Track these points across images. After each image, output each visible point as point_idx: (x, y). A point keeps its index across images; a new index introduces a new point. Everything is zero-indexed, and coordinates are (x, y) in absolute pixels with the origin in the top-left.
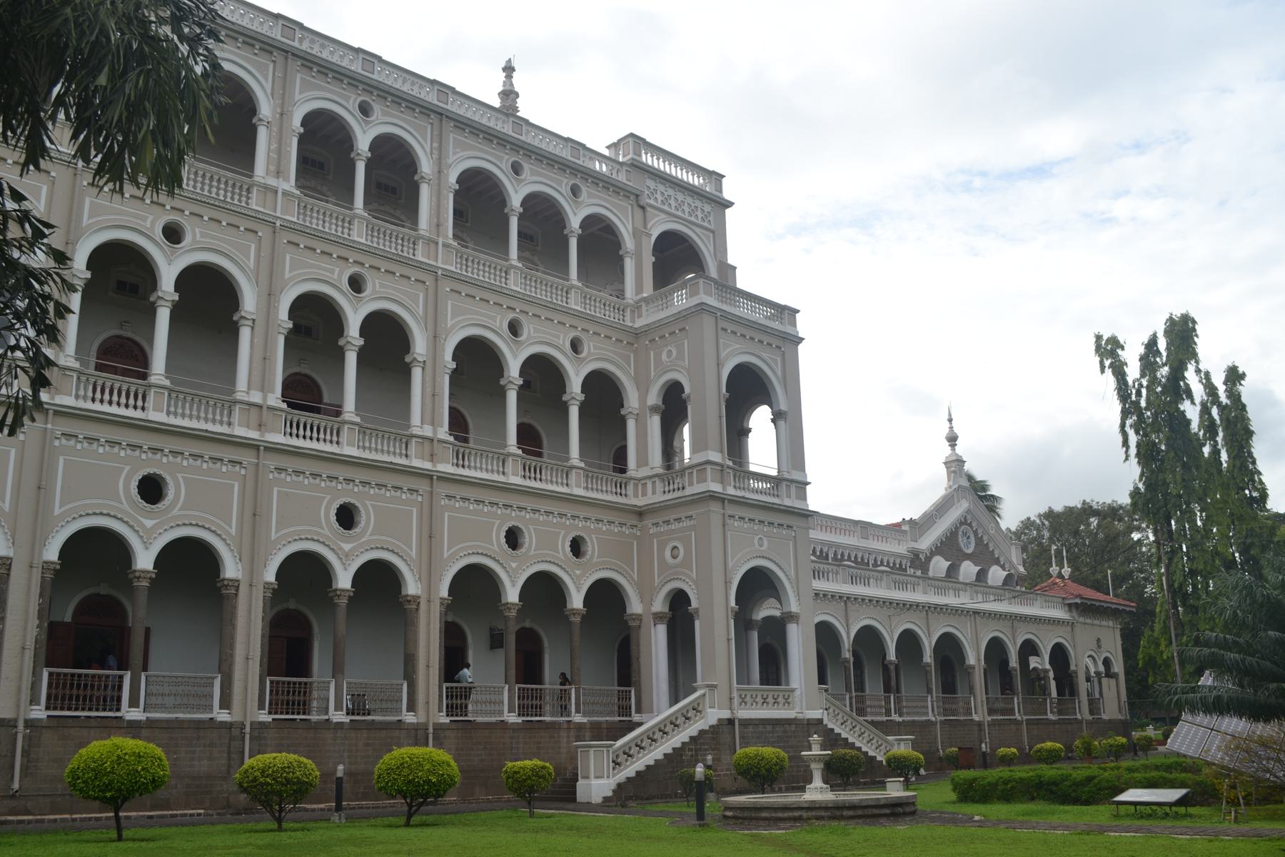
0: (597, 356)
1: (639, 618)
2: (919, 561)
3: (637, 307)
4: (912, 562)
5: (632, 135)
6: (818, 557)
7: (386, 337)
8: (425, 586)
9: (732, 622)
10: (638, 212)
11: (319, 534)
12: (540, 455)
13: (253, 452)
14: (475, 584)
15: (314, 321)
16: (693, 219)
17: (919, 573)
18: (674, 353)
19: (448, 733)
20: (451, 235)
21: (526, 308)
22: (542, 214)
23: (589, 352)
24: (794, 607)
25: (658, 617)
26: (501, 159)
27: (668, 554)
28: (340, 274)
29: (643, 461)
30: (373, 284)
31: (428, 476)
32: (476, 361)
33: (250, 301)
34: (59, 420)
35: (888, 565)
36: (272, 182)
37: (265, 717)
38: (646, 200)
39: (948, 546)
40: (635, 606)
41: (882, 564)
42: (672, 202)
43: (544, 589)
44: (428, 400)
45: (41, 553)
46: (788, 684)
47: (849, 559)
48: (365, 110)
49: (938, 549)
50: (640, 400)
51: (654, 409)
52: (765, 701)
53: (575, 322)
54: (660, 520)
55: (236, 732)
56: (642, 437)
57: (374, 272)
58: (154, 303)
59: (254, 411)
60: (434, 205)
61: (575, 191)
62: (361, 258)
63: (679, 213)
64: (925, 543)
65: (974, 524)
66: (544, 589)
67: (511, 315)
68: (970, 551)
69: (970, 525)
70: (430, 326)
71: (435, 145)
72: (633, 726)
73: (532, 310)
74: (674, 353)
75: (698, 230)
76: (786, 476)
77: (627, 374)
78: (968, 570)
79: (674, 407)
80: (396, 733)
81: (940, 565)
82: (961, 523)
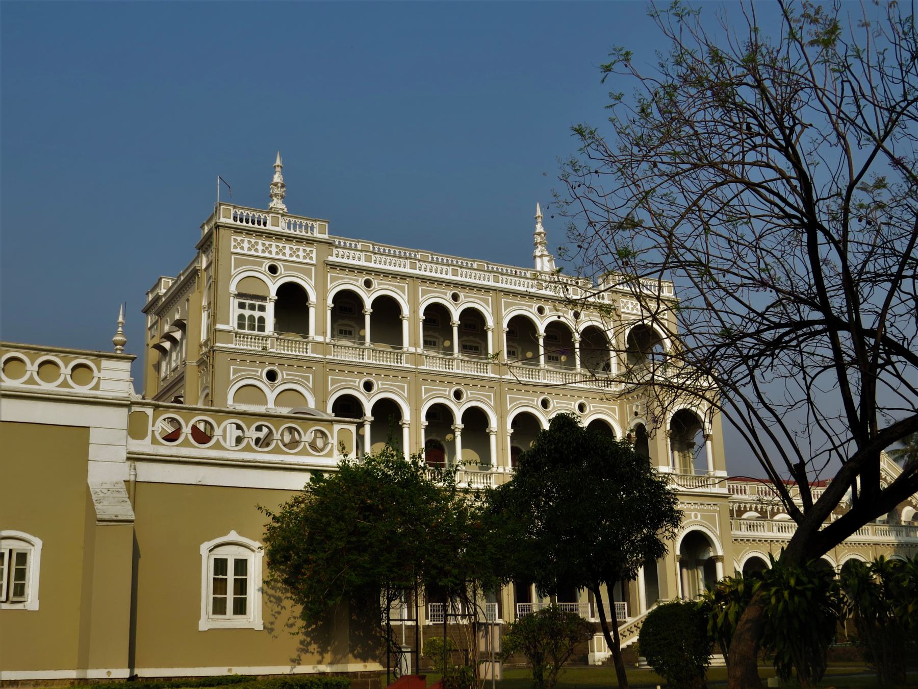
6: (759, 513)
7: (476, 421)
9: (678, 564)
15: (439, 417)
22: (558, 332)
23: (590, 411)
24: (720, 552)
26: (531, 307)
37: (428, 622)
48: (455, 297)
53: (580, 394)
60: (496, 340)
62: (459, 381)
72: (625, 622)
73: (554, 391)
77: (614, 419)
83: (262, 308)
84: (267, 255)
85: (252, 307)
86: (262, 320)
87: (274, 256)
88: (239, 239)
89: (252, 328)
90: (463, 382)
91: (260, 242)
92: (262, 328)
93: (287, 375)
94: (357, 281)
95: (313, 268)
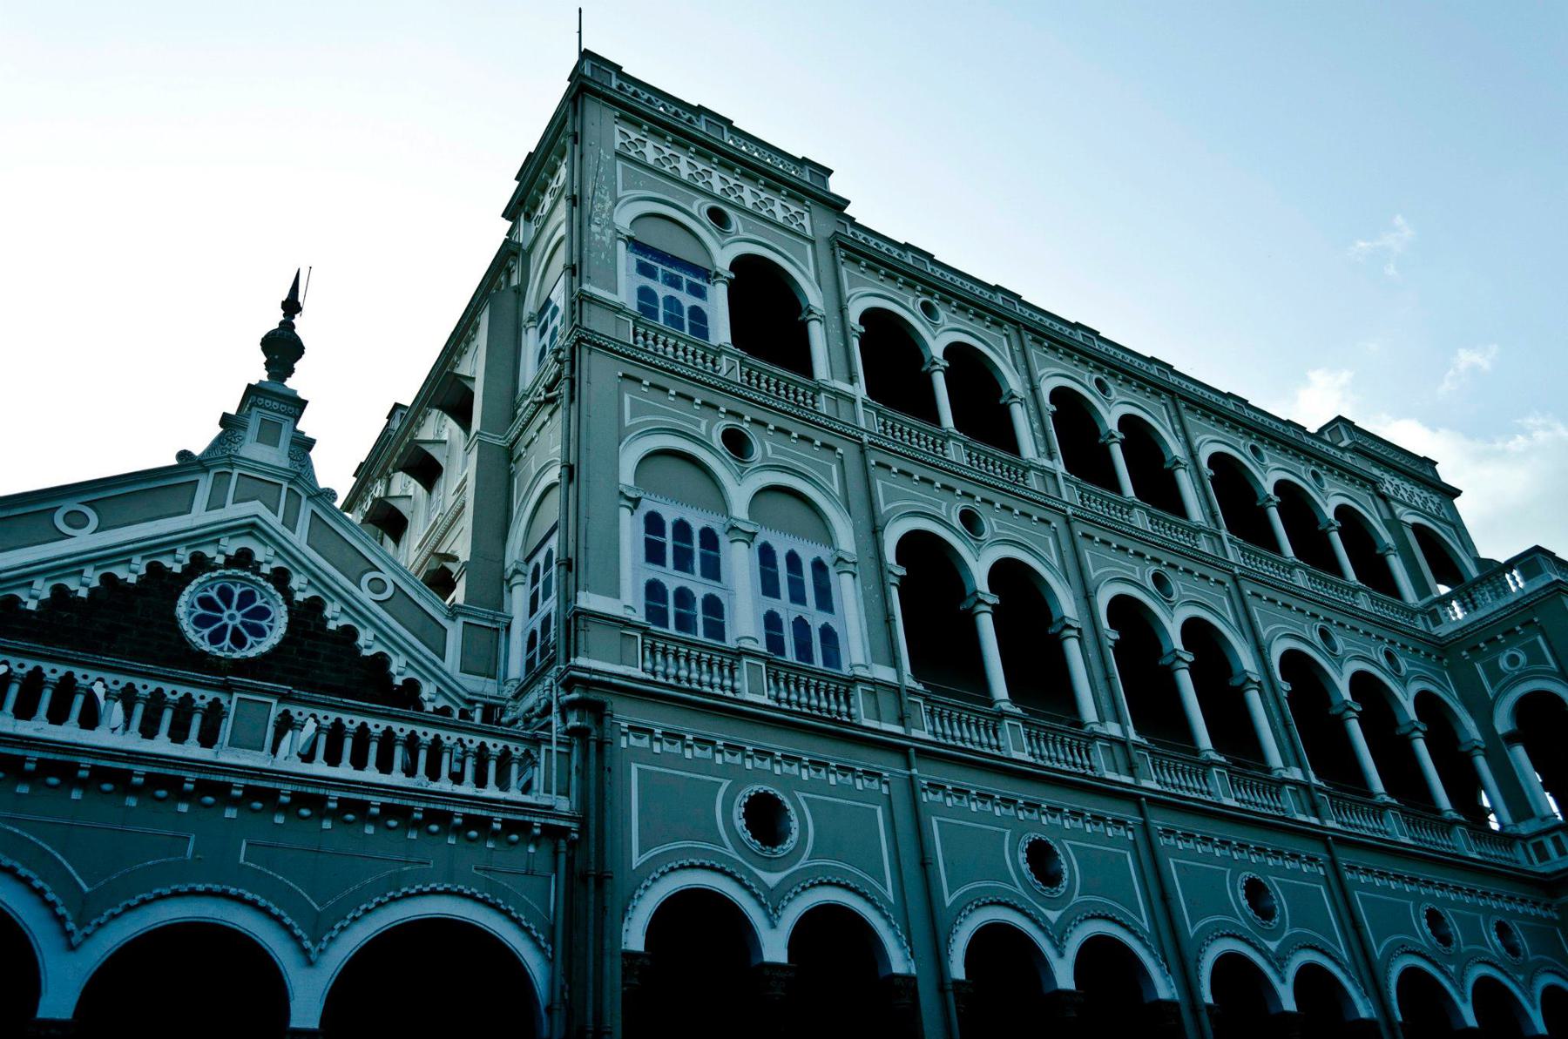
5: (1340, 419)
11: (1237, 927)
18: (1523, 658)
58: (972, 609)
71: (1177, 427)
74: (1523, 658)
95: (809, 247)
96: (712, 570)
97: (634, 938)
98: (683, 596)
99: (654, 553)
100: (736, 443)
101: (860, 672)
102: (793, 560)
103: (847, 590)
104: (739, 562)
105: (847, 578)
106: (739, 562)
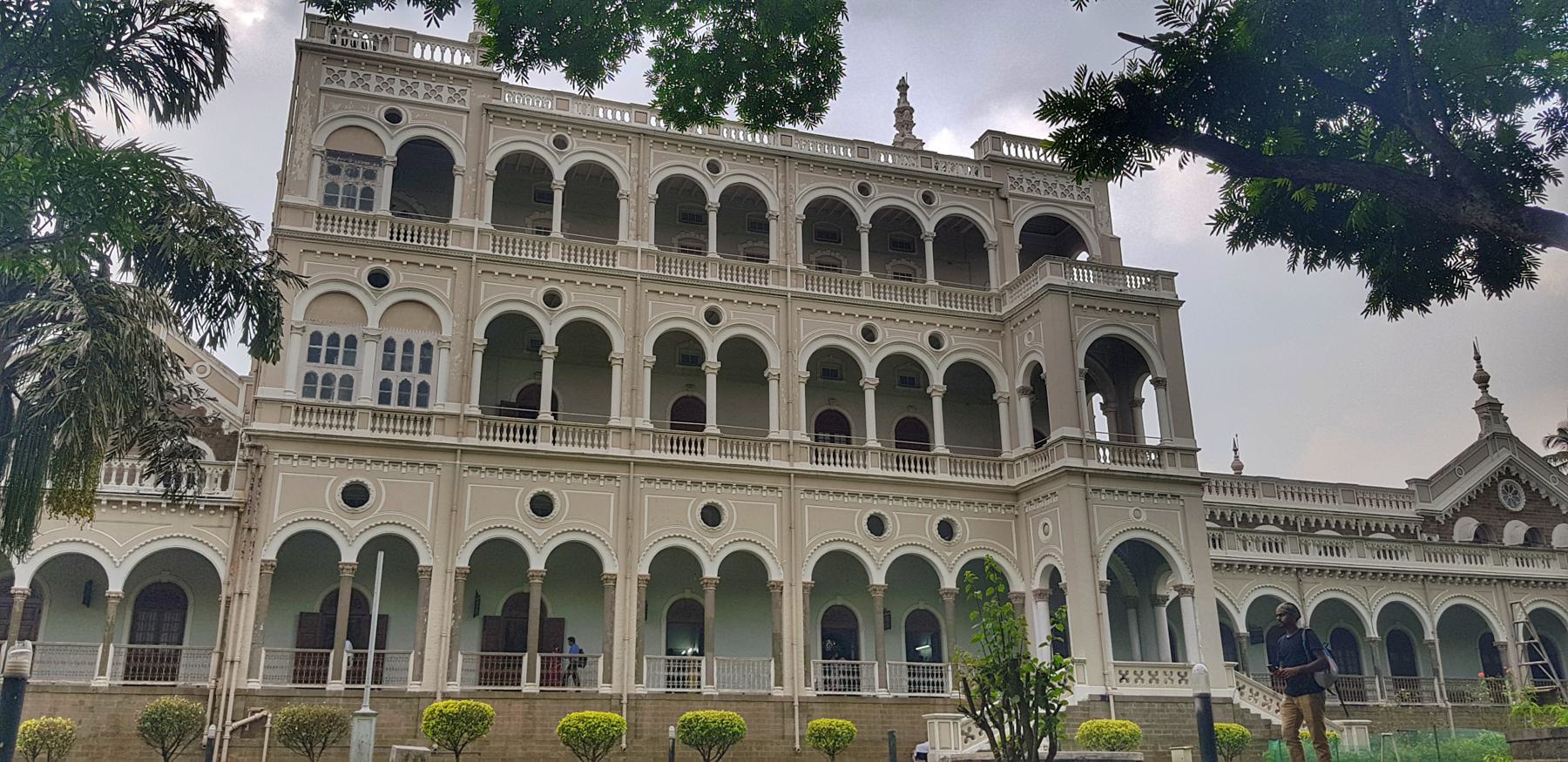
0: (960, 346)
1: (1022, 596)
2: (1435, 527)
3: (1000, 299)
4: (1424, 525)
6: (1282, 527)
8: (792, 574)
10: (1000, 205)
12: (848, 442)
13: (625, 468)
14: (839, 569)
15: (678, 353)
16: (1068, 199)
17: (1436, 539)
19: (816, 706)
20: (800, 260)
21: (878, 313)
24: (1186, 581)
25: (1039, 594)
27: (1041, 531)
28: (697, 311)
29: (1015, 444)
30: (727, 314)
31: (786, 474)
32: (832, 369)
33: (619, 347)
34: (466, 457)
35: (1387, 530)
36: (632, 244)
38: (1007, 190)
39: (1484, 502)
40: (1017, 585)
41: (1378, 529)
42: (1042, 187)
43: (912, 570)
44: (783, 408)
45: (453, 562)
46: (1185, 660)
47: (1328, 526)
48: (714, 168)
49: (1463, 508)
50: (1008, 383)
51: (1023, 391)
52: (1139, 678)
53: (931, 319)
54: (1031, 498)
55: (614, 703)
56: (1016, 418)
57: (728, 305)
59: (625, 434)
61: (928, 198)
63: (1051, 196)
64: (1443, 503)
65: (1522, 477)
66: (912, 570)
67: (864, 323)
68: (1519, 509)
69: (1517, 477)
70: (783, 343)
71: (781, 185)
73: (885, 315)
75: (1073, 209)
76: (1168, 444)
78: (1515, 531)
79: (1037, 387)
80: (764, 705)
81: (1466, 528)
82: (1501, 477)
83: (370, 175)
84: (384, 94)
85: (354, 174)
86: (368, 193)
87: (396, 96)
88: (336, 69)
89: (350, 203)
90: (721, 295)
91: (373, 75)
92: (366, 205)
93: (406, 277)
94: (542, 138)
96: (350, 360)
97: (270, 552)
98: (328, 379)
99: (313, 356)
100: (378, 279)
101: (435, 410)
102: (408, 346)
103: (443, 362)
104: (369, 354)
105: (444, 352)
106: (369, 354)
